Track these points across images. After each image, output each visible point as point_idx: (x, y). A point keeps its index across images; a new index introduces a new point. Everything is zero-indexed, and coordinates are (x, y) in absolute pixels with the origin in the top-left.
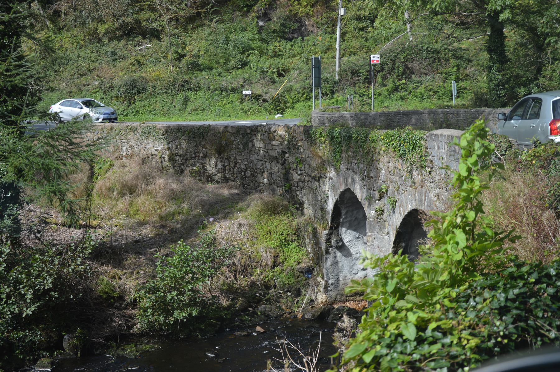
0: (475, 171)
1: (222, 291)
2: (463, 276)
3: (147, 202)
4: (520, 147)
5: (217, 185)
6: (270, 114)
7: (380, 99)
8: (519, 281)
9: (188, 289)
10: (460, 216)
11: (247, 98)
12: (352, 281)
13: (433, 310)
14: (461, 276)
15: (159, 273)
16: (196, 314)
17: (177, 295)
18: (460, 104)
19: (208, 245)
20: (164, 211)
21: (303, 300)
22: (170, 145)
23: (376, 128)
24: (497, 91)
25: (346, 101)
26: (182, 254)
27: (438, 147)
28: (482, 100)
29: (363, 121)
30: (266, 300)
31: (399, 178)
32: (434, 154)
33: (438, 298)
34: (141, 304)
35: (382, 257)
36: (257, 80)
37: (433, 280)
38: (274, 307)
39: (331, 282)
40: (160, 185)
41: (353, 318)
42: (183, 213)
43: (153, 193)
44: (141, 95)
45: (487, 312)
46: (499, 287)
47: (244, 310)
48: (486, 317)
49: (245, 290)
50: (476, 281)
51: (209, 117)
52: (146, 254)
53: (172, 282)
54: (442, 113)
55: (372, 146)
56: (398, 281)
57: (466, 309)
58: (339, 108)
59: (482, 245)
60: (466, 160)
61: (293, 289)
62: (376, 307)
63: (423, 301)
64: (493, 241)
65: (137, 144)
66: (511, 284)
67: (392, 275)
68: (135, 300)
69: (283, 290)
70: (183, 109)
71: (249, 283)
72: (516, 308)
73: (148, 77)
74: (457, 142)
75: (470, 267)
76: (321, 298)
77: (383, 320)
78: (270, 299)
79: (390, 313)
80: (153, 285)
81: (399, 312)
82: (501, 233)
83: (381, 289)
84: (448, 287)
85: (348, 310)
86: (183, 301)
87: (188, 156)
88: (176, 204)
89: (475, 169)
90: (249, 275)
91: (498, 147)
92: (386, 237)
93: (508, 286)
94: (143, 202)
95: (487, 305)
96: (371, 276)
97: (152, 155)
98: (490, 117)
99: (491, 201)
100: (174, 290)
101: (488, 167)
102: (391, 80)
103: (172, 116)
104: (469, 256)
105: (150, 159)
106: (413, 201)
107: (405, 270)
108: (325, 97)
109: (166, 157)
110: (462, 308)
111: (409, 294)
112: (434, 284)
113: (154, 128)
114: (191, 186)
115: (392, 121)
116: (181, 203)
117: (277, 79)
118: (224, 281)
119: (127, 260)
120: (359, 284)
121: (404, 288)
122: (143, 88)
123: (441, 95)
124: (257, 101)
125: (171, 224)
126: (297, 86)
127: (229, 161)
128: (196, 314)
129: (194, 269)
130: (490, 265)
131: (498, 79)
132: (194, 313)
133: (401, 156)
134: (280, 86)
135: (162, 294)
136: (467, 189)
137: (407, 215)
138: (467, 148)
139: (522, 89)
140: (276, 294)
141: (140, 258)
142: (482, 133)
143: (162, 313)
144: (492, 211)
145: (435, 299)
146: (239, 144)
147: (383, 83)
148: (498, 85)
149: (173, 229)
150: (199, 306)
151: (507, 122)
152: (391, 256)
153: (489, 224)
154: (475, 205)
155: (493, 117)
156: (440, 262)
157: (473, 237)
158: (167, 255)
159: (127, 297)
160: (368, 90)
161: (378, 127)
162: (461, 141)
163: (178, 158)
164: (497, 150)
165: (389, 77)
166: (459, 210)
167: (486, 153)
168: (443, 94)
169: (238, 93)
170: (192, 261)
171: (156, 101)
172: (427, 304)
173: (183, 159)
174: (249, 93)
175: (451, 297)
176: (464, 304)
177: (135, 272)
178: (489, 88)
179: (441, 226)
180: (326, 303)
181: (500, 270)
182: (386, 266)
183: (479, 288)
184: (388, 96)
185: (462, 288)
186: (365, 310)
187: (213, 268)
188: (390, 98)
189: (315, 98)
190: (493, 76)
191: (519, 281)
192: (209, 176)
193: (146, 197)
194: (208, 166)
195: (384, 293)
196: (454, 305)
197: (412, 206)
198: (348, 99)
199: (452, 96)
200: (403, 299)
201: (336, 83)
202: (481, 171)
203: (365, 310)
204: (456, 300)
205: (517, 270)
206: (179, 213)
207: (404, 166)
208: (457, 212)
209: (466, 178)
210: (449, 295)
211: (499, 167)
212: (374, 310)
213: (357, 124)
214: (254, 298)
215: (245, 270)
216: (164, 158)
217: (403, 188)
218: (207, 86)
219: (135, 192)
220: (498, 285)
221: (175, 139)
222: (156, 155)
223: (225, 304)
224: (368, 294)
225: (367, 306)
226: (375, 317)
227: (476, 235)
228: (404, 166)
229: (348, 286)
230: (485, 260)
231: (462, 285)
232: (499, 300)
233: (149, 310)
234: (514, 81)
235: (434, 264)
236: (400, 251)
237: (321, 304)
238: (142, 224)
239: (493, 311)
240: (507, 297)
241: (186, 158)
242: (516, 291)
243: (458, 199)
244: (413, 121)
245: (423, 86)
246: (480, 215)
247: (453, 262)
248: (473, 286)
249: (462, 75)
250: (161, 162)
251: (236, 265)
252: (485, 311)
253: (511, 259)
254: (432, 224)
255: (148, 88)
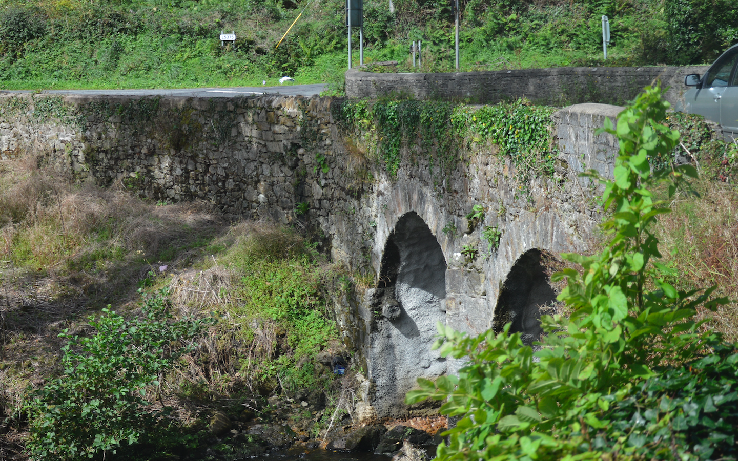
0: (643, 180)
1: (182, 399)
2: (621, 371)
3: (45, 237)
4: (725, 136)
5: (173, 206)
6: (270, 76)
7: (470, 50)
8: (723, 381)
9: (121, 395)
10: (616, 262)
11: (227, 47)
12: (420, 380)
13: (566, 433)
14: (618, 372)
15: (68, 366)
16: (136, 440)
17: (100, 407)
18: (617, 57)
19: (156, 315)
20: (76, 254)
21: (329, 415)
22: (88, 133)
23: (464, 101)
24: (683, 33)
25: (409, 53)
26: (109, 332)
27: (577, 136)
28: (656, 50)
29: (440, 89)
30: (262, 416)
31: (506, 192)
32: (568, 149)
33: (575, 411)
34: (35, 422)
35: (474, 336)
36: (245, 15)
37: (566, 379)
38: (276, 428)
39: (381, 381)
40: (69, 206)
41: (421, 447)
42: (111, 256)
43: (57, 220)
44: (35, 41)
45: (666, 437)
46: (687, 392)
47: (223, 433)
48: (663, 447)
49: (225, 397)
50: (645, 381)
51: (159, 81)
52: (43, 332)
53: (91, 383)
54: (585, 74)
55: (455, 134)
56: (504, 381)
57: (627, 432)
58: (396, 64)
59: (656, 314)
60: (628, 160)
61: (312, 395)
62: (463, 428)
63: (549, 416)
64: (677, 308)
65: (27, 132)
66: (709, 386)
67: (493, 369)
68: (24, 415)
69: (294, 397)
70: (111, 68)
71: (231, 384)
72: (720, 430)
73: (47, 9)
74: (611, 126)
75: (634, 356)
76: (364, 411)
77: (475, 452)
78: (269, 412)
79: (488, 440)
80: (57, 388)
81: (504, 436)
82: (691, 293)
83: (472, 395)
84: (594, 392)
85: (412, 434)
86: (111, 418)
87: (121, 153)
88: (98, 241)
89: (645, 176)
90: (232, 370)
91: (685, 136)
92: (482, 301)
93: (704, 389)
94: (39, 238)
95: (665, 425)
96: (455, 371)
97: (55, 151)
98: (672, 81)
99: (672, 235)
100: (96, 397)
101: (668, 173)
102: (491, 14)
103: (90, 79)
104: (633, 336)
105: (51, 159)
106: (531, 235)
107: (516, 359)
108: (370, 44)
109: (81, 154)
110: (620, 430)
111: (523, 404)
112: (569, 387)
113: (58, 101)
114: (125, 207)
115: (492, 89)
116: (107, 238)
117: (282, 12)
118: (186, 381)
119: (8, 342)
120: (433, 386)
121: (514, 393)
122: (39, 29)
123: (582, 42)
124: (246, 52)
125: (88, 276)
126: (319, 25)
127: (196, 162)
128: (136, 440)
129: (131, 359)
130: (672, 352)
131: (685, 12)
132: (132, 440)
133: (508, 152)
134: (289, 25)
135: (73, 405)
136: (629, 213)
137: (519, 261)
138: (629, 138)
139: (730, 31)
140: (280, 405)
141: (33, 339)
142: (657, 110)
143: (72, 439)
144: (675, 252)
145: (570, 414)
146: (213, 131)
147: (475, 20)
148: (686, 24)
149: (92, 286)
150: (140, 426)
151: (702, 90)
152: (490, 335)
153: (670, 277)
154: (644, 242)
155: (677, 82)
156: (580, 346)
157: (641, 301)
158: (82, 334)
159: (10, 410)
160: (448, 32)
161: (467, 100)
162: (618, 125)
163: (102, 156)
164: (685, 142)
165: (488, 9)
166: (614, 251)
167: (664, 148)
168: (585, 40)
169: (211, 37)
170: (127, 344)
171: (63, 53)
172: (557, 423)
173: (111, 158)
174: (232, 37)
175: (600, 409)
176: (624, 422)
177: (23, 365)
178: (669, 28)
179: (581, 281)
180: (372, 421)
181: (688, 360)
182: (482, 353)
183: (650, 393)
184: (485, 43)
185: (620, 393)
186: (443, 434)
187: (167, 357)
188: (489, 47)
189: (352, 47)
190: (676, 6)
191: (723, 381)
192: (159, 189)
193: (45, 228)
194: (157, 171)
195: (478, 403)
196: (605, 424)
197: (528, 244)
198: (411, 48)
199: (601, 43)
200: (513, 414)
201: (390, 19)
202: (654, 179)
203: (443, 434)
204: (609, 415)
205: (721, 361)
206: (104, 257)
207: (515, 170)
208: (611, 256)
209: (627, 192)
210: (597, 405)
211: (687, 173)
212: (459, 434)
213: (428, 93)
214: (240, 412)
215: (224, 360)
216: (76, 156)
217: (512, 210)
218: (155, 26)
219: (23, 218)
220: (685, 389)
221: (97, 121)
222: (62, 151)
223: (187, 422)
224: (449, 405)
225: (446, 426)
226: (460, 447)
227: (646, 297)
228: (515, 170)
229: (413, 389)
230: (662, 341)
231: (619, 388)
232: (688, 416)
233: (49, 434)
234: (714, 15)
235: (569, 350)
236: (507, 327)
237: (363, 422)
238: (37, 277)
239: (677, 435)
240: (702, 410)
241: (117, 157)
242: (719, 399)
243: (613, 230)
244: (531, 88)
245: (549, 25)
246: (652, 259)
247: (604, 346)
248: (639, 389)
249: (620, 6)
250: (72, 164)
251: (207, 351)
252: (662, 436)
253: (709, 340)
254: (565, 276)
255: (48, 28)
